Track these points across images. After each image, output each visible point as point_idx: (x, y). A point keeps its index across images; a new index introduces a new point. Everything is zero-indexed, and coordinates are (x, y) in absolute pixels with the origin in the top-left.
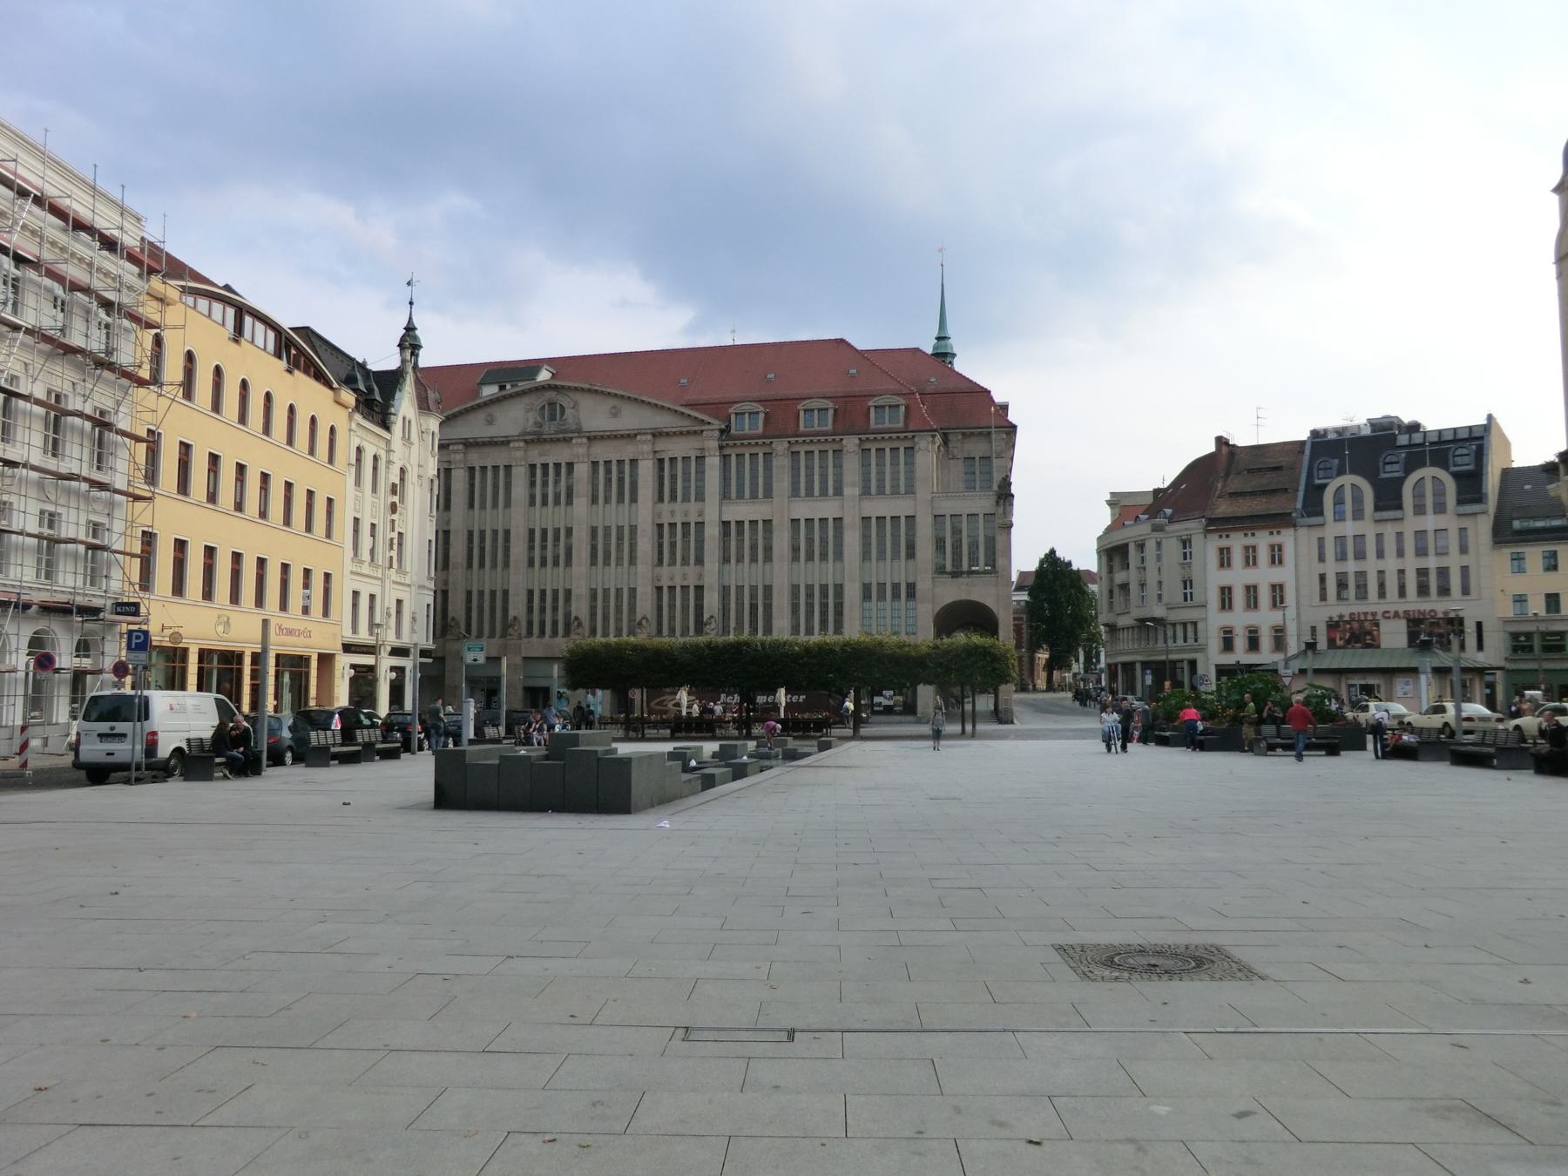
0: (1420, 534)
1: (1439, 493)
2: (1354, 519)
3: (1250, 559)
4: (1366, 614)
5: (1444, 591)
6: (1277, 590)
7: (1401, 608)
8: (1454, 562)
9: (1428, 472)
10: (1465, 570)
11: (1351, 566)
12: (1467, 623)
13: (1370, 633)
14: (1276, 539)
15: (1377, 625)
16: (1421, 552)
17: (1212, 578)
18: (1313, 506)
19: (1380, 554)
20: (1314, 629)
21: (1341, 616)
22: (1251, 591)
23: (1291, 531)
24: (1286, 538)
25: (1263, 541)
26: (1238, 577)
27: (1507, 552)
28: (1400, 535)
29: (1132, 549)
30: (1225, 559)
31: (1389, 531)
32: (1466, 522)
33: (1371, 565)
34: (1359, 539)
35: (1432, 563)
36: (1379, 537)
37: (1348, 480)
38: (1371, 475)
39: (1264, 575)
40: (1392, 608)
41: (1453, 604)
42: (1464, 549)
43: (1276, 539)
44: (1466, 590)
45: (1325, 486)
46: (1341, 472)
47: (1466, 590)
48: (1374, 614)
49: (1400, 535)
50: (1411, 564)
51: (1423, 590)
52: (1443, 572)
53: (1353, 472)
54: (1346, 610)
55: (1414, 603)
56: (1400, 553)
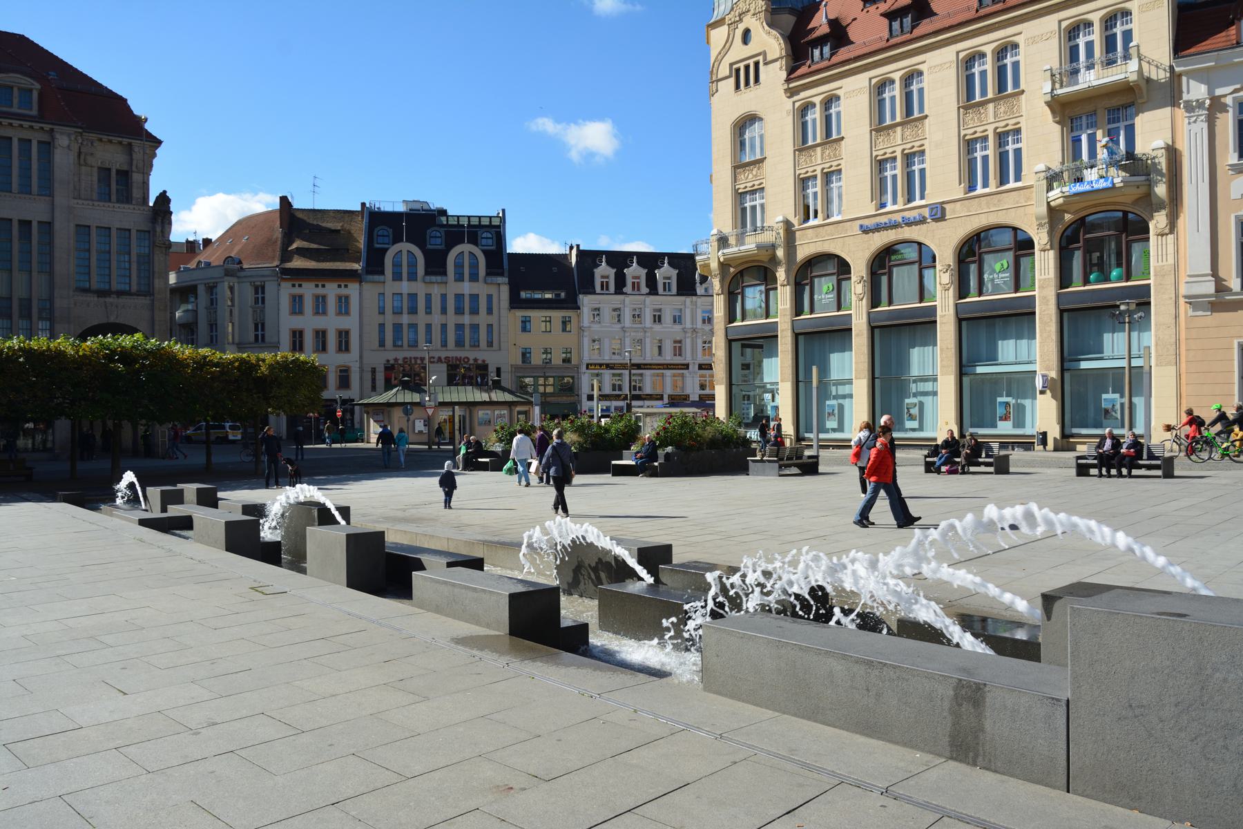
0: (459, 297)
1: (474, 266)
2: (409, 280)
3: (320, 305)
4: (416, 358)
5: (475, 345)
6: (344, 336)
7: (443, 355)
8: (482, 319)
9: (466, 248)
10: (490, 326)
11: (467, 319)
12: (490, 369)
13: (418, 375)
14: (343, 291)
15: (424, 368)
16: (459, 311)
17: (288, 322)
18: (375, 264)
19: (429, 310)
20: (374, 371)
21: (396, 360)
22: (321, 335)
23: (356, 285)
24: (353, 290)
25: (332, 290)
26: (309, 322)
27: (520, 313)
28: (444, 297)
29: (201, 290)
30: (297, 305)
31: (436, 291)
32: (492, 290)
33: (421, 319)
34: (413, 297)
35: (467, 319)
36: (428, 297)
37: (405, 246)
38: (421, 245)
39: (332, 323)
40: (437, 355)
41: (482, 355)
42: (490, 311)
43: (343, 291)
44: (490, 344)
45: (386, 250)
46: (397, 239)
47: (490, 344)
48: (422, 359)
49: (444, 297)
50: (452, 319)
51: (460, 343)
52: (475, 328)
53: (407, 241)
54: (401, 355)
55: (453, 352)
56: (444, 311)
